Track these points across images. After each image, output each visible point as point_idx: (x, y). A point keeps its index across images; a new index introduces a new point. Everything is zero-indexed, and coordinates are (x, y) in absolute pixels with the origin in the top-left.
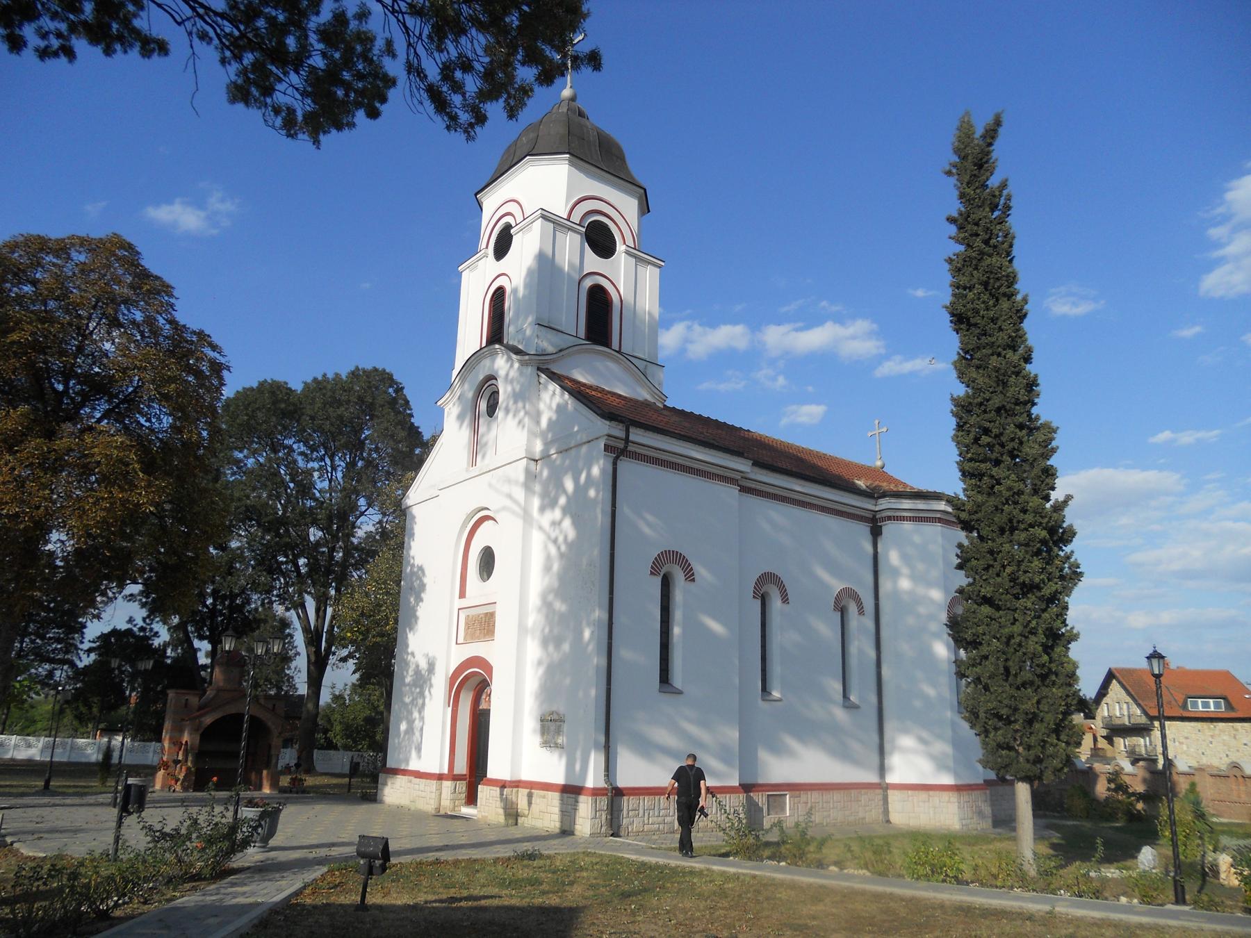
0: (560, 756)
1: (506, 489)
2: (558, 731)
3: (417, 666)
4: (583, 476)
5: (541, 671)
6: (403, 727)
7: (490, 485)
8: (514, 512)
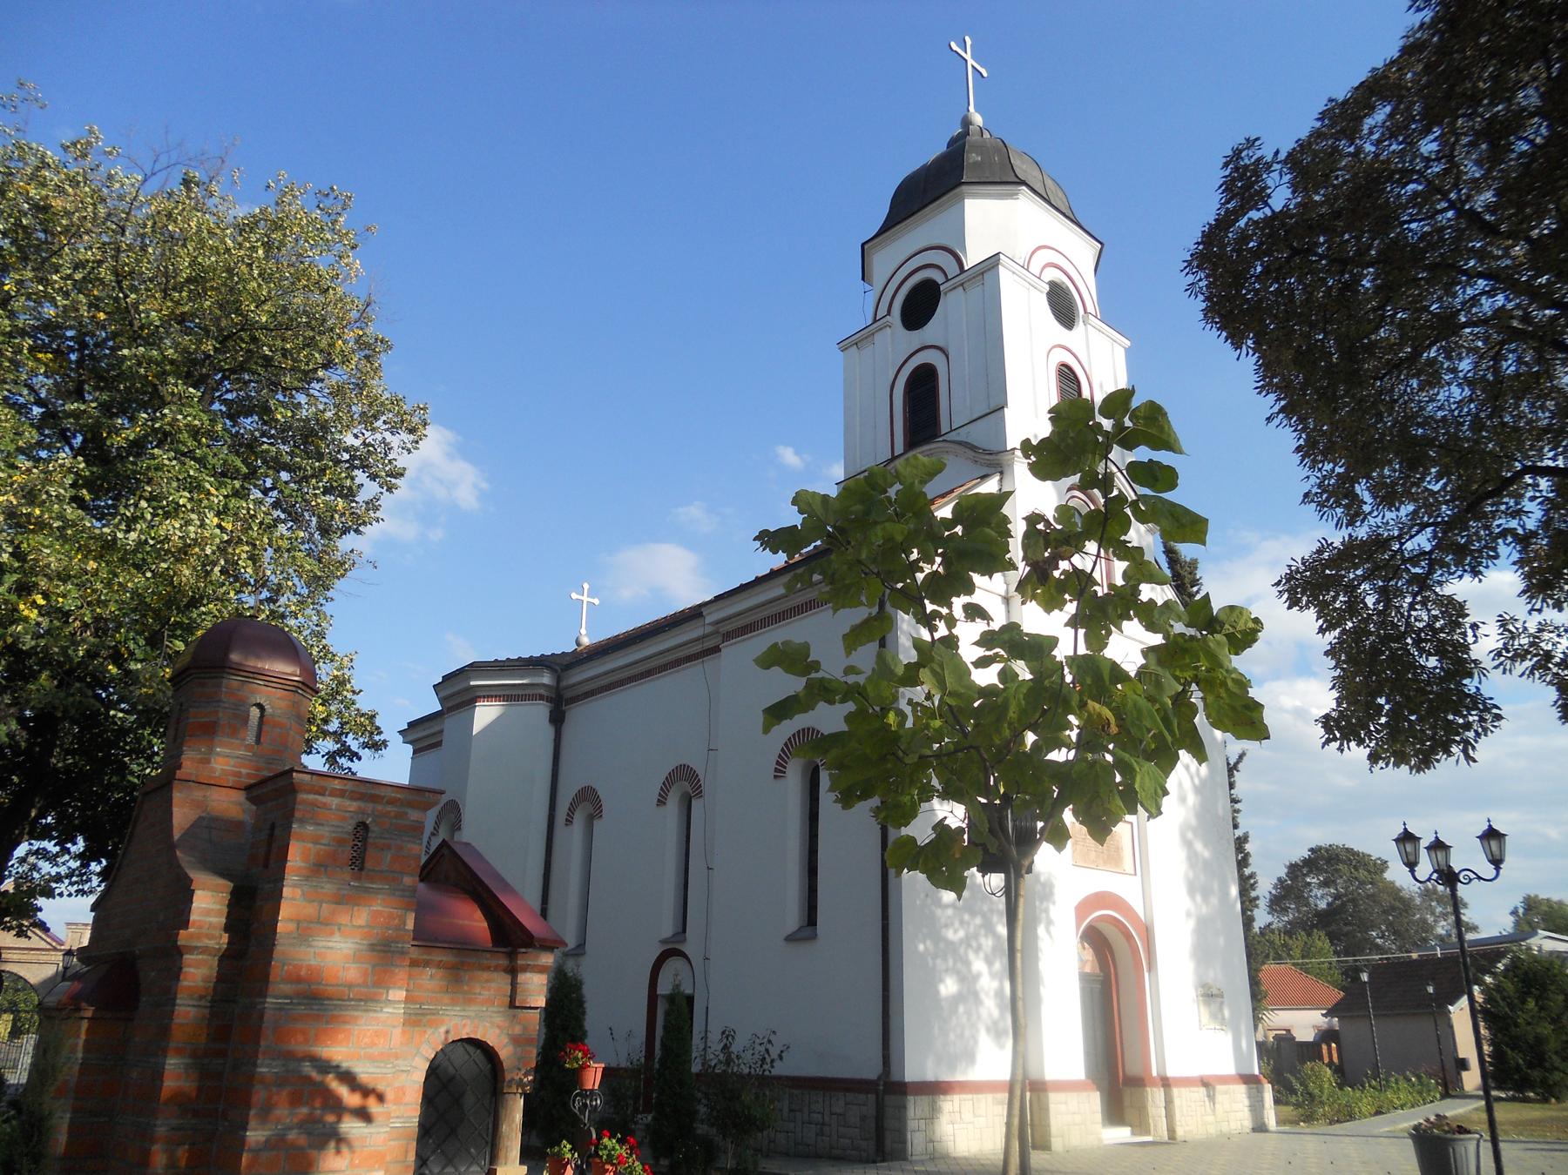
5: (1191, 924)
6: (949, 987)
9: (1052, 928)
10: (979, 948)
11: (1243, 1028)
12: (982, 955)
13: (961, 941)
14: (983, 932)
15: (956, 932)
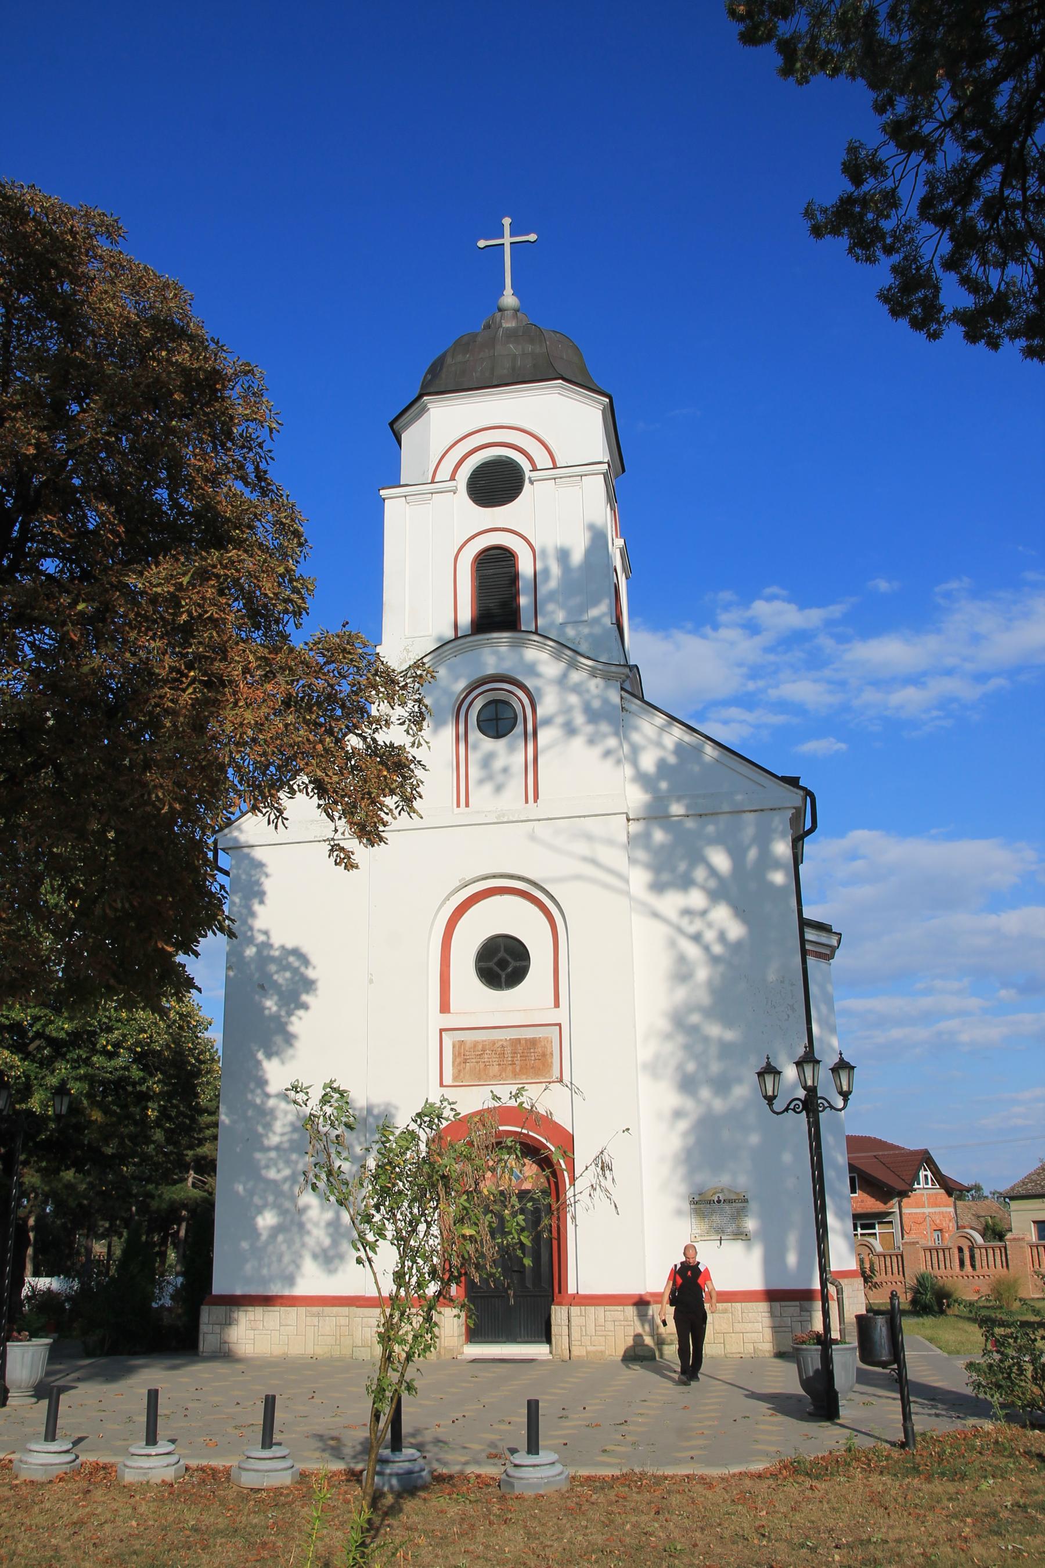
0: (749, 1248)
1: (582, 848)
2: (739, 1215)
5: (683, 1125)
6: (267, 1220)
7: (533, 837)
8: (606, 886)
11: (792, 1239)
13: (286, 1179)
15: (279, 1171)
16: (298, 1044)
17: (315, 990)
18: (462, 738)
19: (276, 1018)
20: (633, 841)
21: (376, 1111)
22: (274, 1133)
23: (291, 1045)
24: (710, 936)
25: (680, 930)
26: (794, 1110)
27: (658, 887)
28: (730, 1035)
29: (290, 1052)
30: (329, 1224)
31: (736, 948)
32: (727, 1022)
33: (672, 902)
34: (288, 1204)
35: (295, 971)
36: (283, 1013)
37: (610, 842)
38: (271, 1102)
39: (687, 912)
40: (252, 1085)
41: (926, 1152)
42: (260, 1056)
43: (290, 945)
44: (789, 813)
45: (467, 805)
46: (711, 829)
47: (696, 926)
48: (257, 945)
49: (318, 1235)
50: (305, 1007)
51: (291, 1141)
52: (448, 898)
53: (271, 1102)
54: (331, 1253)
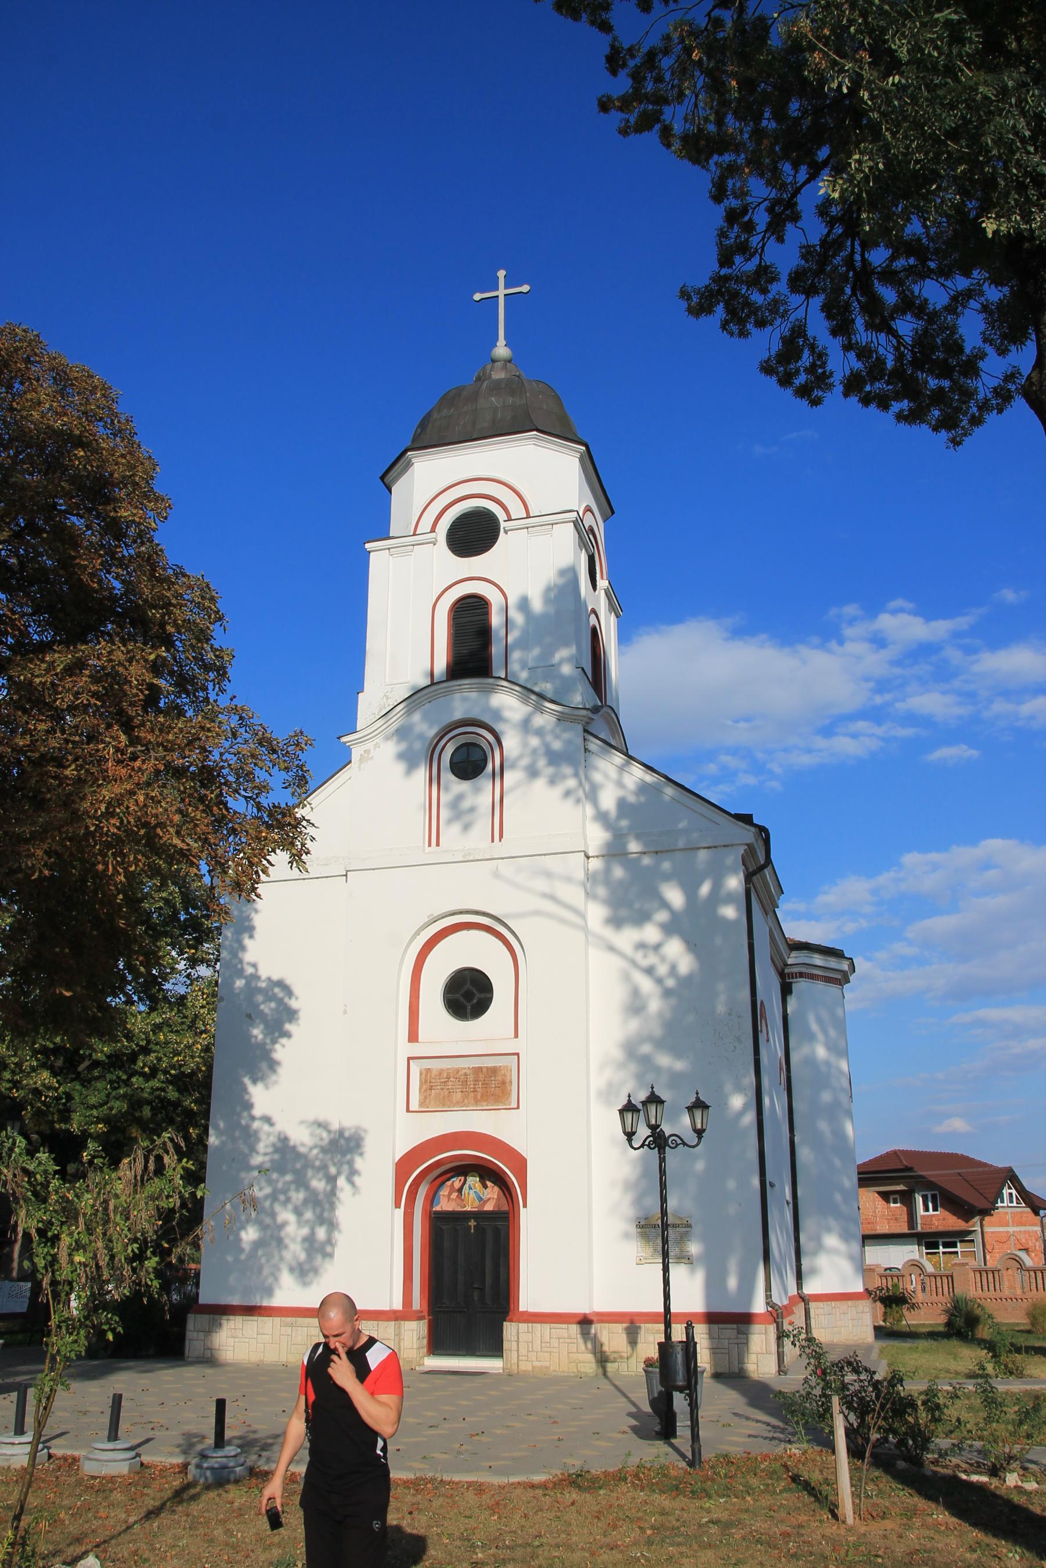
0: (692, 1272)
1: (541, 884)
3: (284, 1140)
4: (705, 889)
6: (250, 1235)
7: (496, 875)
8: (563, 921)
9: (356, 1179)
10: (288, 1200)
12: (290, 1207)
13: (267, 1197)
14: (293, 1187)
15: (261, 1189)
16: (281, 1070)
17: (298, 1019)
18: (435, 779)
19: (262, 1046)
20: (591, 877)
21: (347, 1134)
22: (258, 1153)
23: (275, 1071)
24: (662, 970)
25: (634, 963)
26: (648, 1146)
27: (616, 922)
28: (679, 1065)
29: (274, 1077)
30: (305, 1240)
31: (685, 982)
32: (678, 1054)
33: (627, 938)
34: (268, 1220)
35: (280, 1001)
36: (268, 1041)
37: (568, 879)
38: (256, 1125)
39: (641, 946)
40: (238, 1109)
41: (1010, 1170)
42: (247, 1081)
43: (275, 977)
44: (741, 850)
45: (438, 844)
46: (666, 866)
47: (652, 959)
48: (246, 978)
49: (295, 1250)
50: (288, 1035)
51: (272, 1161)
52: (418, 933)
53: (256, 1125)
54: (306, 1267)
